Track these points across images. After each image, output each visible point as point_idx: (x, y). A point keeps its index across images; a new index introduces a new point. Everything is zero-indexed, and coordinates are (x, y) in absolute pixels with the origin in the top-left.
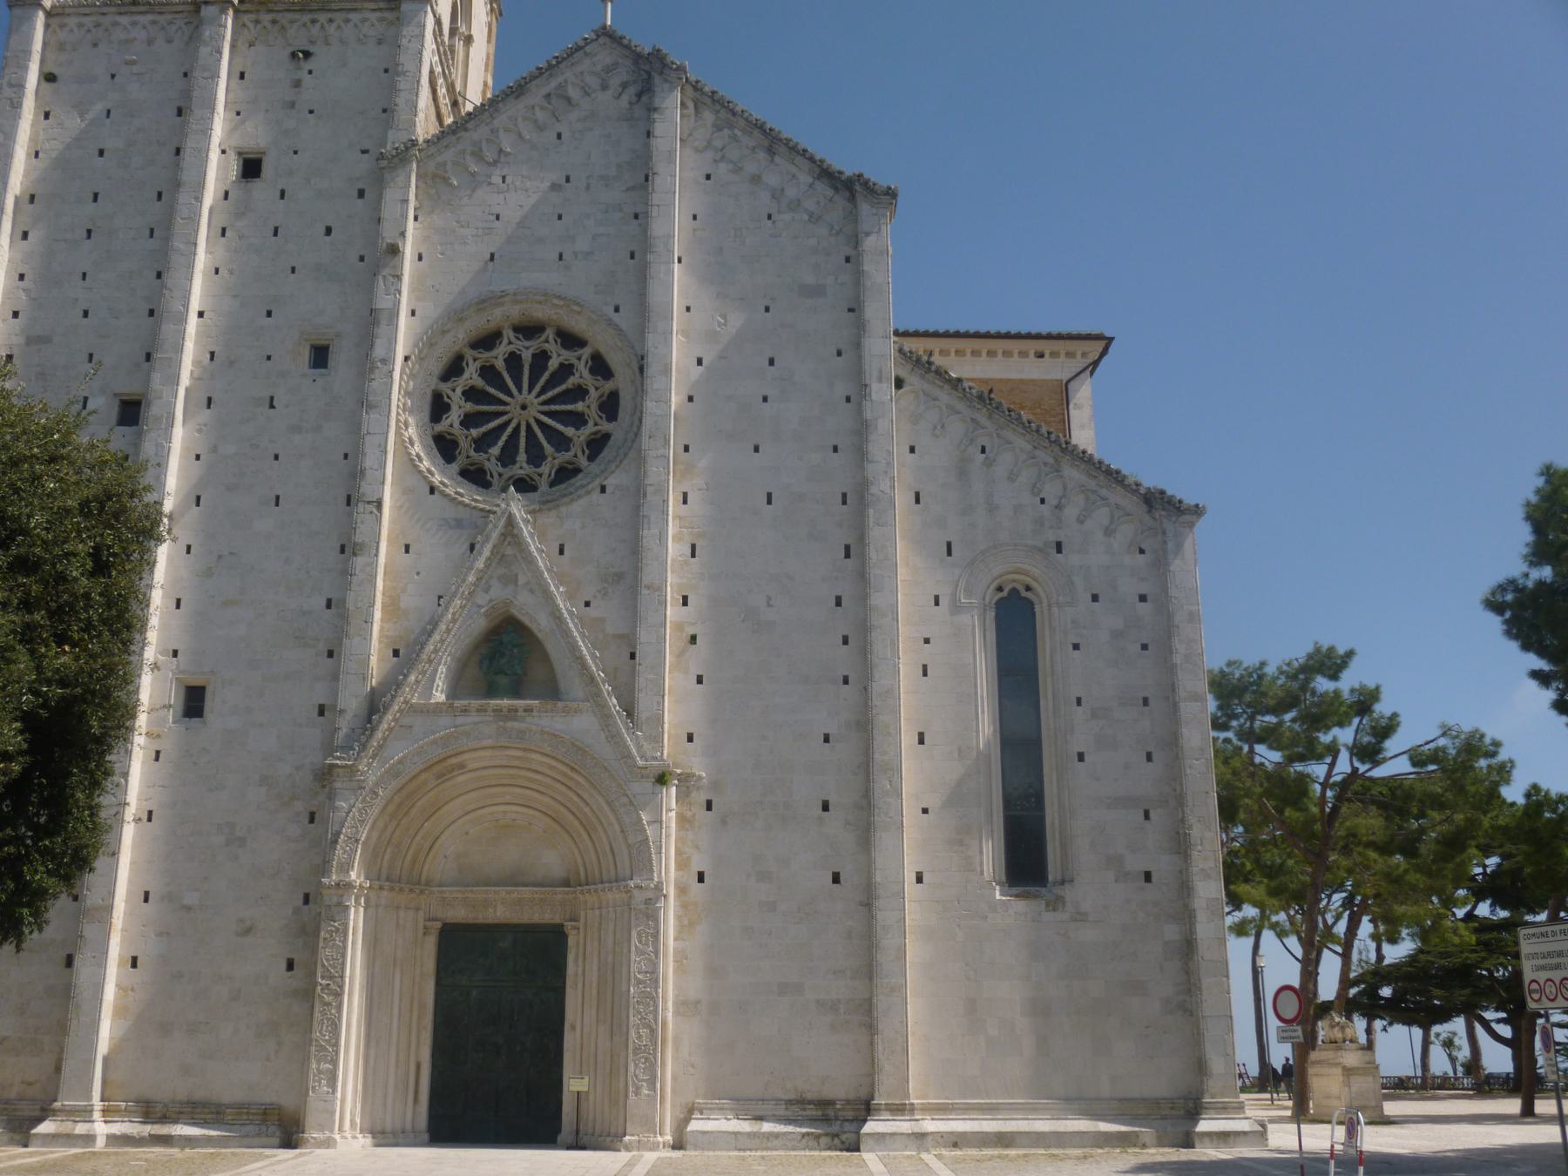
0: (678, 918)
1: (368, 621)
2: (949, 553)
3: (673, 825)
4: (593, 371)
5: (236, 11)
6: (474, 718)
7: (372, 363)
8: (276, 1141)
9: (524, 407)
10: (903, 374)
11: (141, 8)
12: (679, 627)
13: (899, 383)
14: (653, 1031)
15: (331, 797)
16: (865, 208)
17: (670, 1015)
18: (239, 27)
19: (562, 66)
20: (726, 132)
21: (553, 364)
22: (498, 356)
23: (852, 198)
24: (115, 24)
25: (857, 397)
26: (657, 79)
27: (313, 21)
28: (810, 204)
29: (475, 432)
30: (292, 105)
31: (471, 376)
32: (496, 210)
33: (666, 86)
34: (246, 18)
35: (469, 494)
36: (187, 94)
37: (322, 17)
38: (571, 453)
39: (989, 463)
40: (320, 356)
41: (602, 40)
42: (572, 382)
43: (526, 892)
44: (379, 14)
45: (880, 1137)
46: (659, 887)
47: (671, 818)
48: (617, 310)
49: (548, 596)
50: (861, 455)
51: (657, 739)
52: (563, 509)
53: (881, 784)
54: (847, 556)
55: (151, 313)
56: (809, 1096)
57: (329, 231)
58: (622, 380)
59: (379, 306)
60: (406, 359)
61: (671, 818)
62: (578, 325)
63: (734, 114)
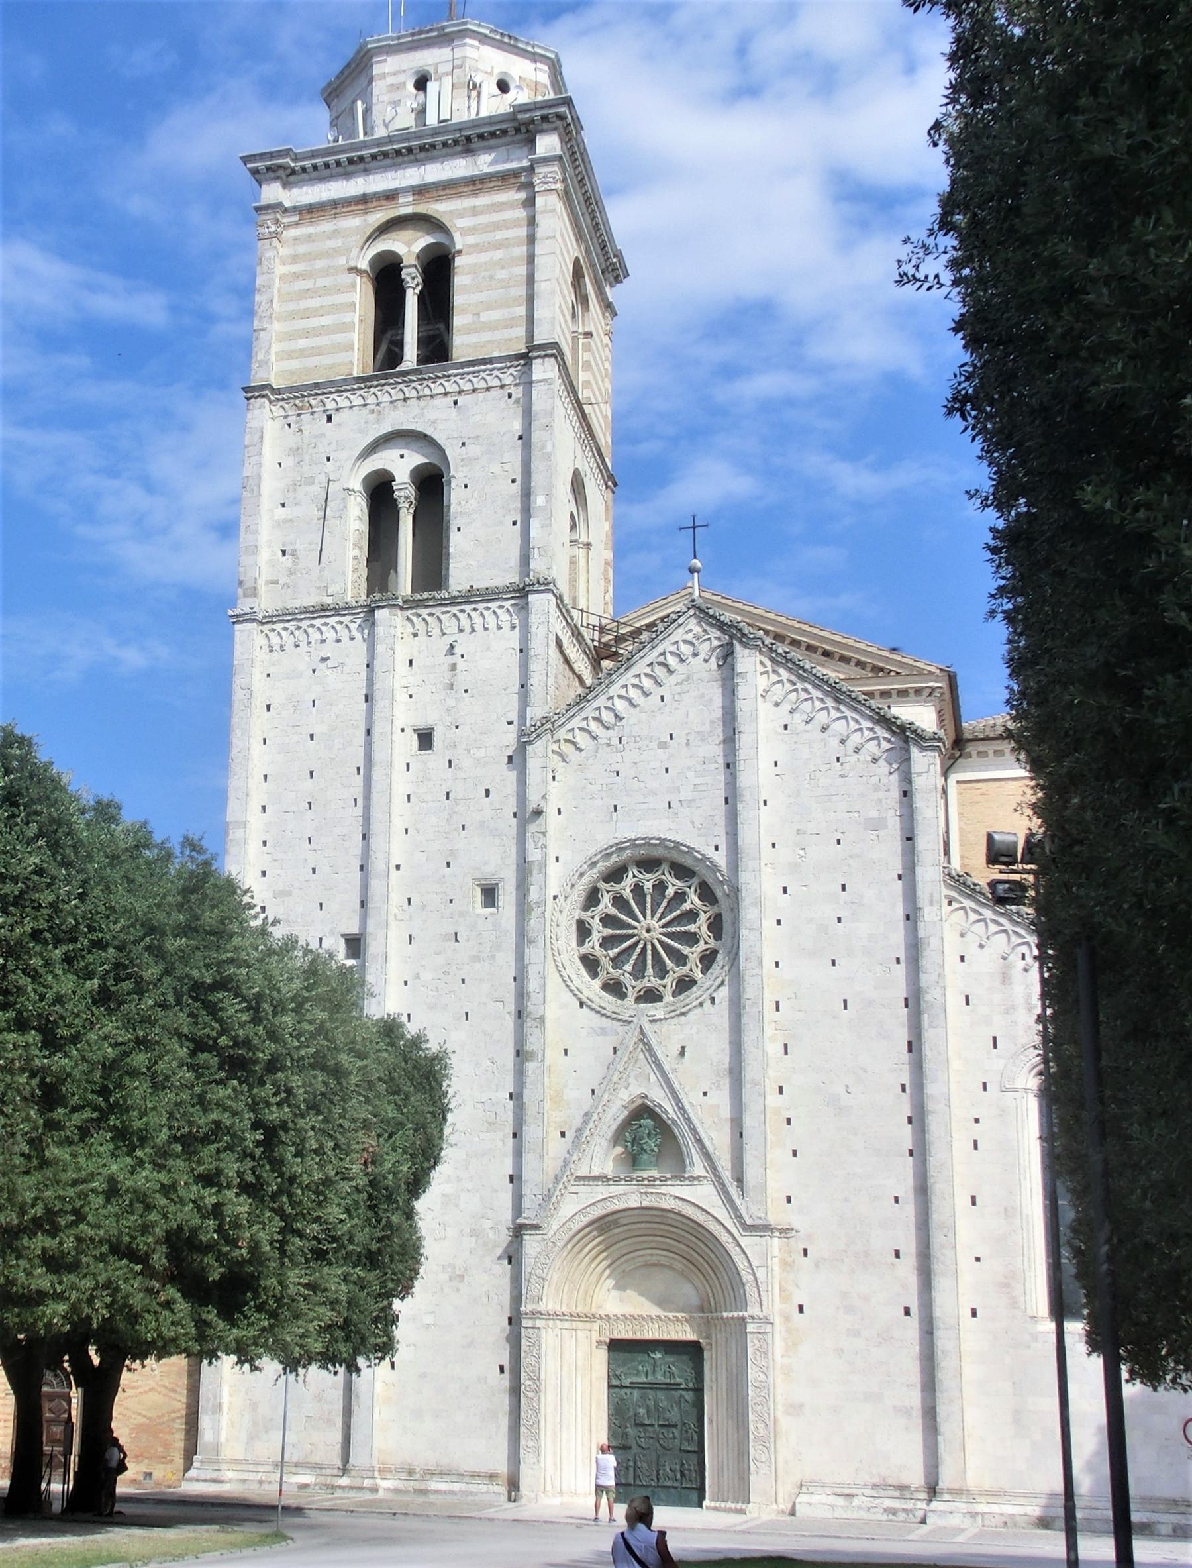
7: (529, 904)
26: (738, 647)
29: (612, 953)
30: (451, 686)
31: (606, 904)
32: (616, 768)
38: (687, 968)
41: (692, 612)
44: (512, 602)
56: (890, 1481)
58: (724, 905)
59: (531, 859)
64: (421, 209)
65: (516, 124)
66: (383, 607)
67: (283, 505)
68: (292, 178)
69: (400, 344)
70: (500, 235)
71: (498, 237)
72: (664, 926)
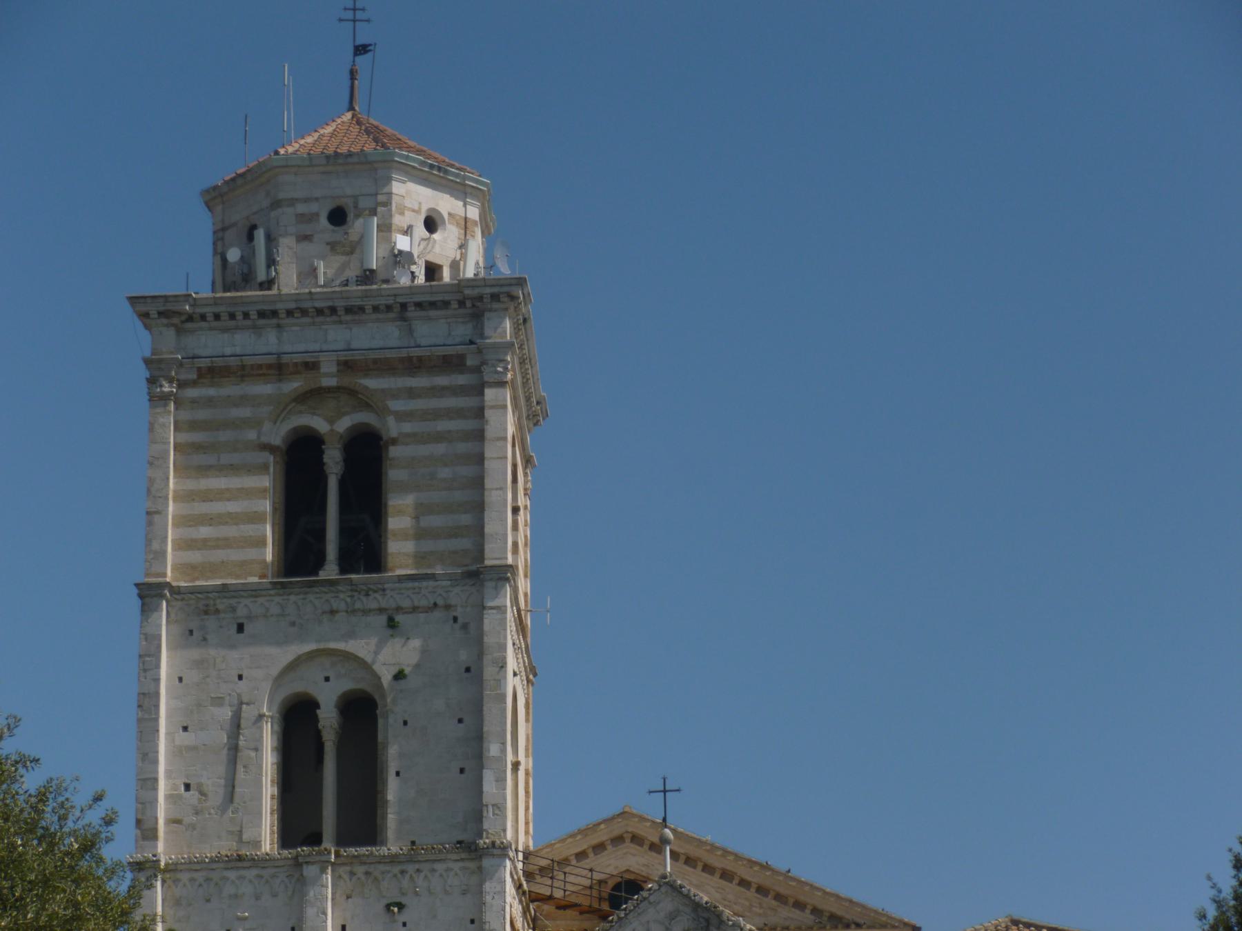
5: (333, 864)
11: (246, 864)
18: (337, 879)
19: (630, 917)
24: (225, 879)
34: (343, 871)
37: (411, 868)
44: (461, 864)
66: (313, 863)
67: (185, 729)
68: (189, 325)
69: (321, 535)
70: (443, 425)
71: (439, 428)
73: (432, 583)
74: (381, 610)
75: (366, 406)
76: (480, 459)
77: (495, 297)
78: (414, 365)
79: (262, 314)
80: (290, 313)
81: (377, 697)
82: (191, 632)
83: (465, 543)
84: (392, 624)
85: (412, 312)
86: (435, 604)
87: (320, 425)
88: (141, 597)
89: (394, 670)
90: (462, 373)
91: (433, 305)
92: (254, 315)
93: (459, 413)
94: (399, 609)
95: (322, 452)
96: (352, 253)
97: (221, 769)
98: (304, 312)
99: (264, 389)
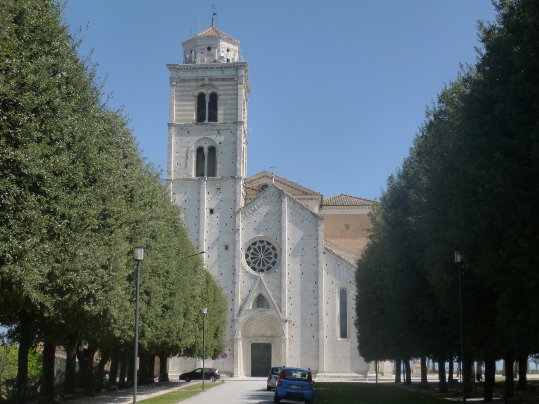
0: (289, 343)
1: (238, 295)
2: (332, 283)
3: (288, 328)
4: (273, 249)
6: (256, 312)
8: (229, 376)
9: (261, 256)
10: (325, 251)
12: (288, 296)
13: (324, 253)
14: (285, 360)
15: (234, 324)
16: (319, 221)
17: (288, 358)
20: (295, 205)
21: (266, 248)
22: (256, 247)
23: (317, 218)
24: (185, 183)
25: (317, 256)
26: (282, 196)
27: (220, 182)
28: (310, 219)
29: (253, 261)
31: (252, 250)
32: (255, 220)
33: (284, 197)
34: (208, 182)
35: (253, 272)
36: (200, 197)
37: (222, 181)
39: (339, 267)
40: (227, 248)
42: (269, 251)
43: (265, 338)
45: (319, 376)
46: (286, 338)
47: (287, 327)
48: (277, 239)
49: (267, 292)
50: (317, 266)
51: (285, 315)
52: (269, 276)
53: (320, 322)
54: (315, 283)
55: (197, 240)
57: (226, 224)
58: (278, 251)
60: (241, 248)
61: (287, 327)
62: (270, 242)
63: (296, 202)
64: (211, 83)
65: (234, 66)
67: (177, 153)
68: (179, 71)
69: (205, 114)
70: (230, 92)
72: (265, 255)
73: (227, 125)
74: (217, 130)
75: (214, 88)
76: (237, 99)
77: (241, 66)
78: (224, 80)
79: (193, 69)
80: (199, 68)
81: (216, 147)
82: (178, 133)
83: (234, 117)
84: (219, 132)
85: (224, 69)
86: (228, 129)
87: (204, 91)
88: (168, 126)
89: (219, 142)
90: (234, 81)
91: (228, 67)
92: (192, 69)
93: (233, 90)
94: (220, 130)
95: (205, 97)
96: (212, 56)
97: (184, 160)
98: (202, 68)
99: (194, 84)
